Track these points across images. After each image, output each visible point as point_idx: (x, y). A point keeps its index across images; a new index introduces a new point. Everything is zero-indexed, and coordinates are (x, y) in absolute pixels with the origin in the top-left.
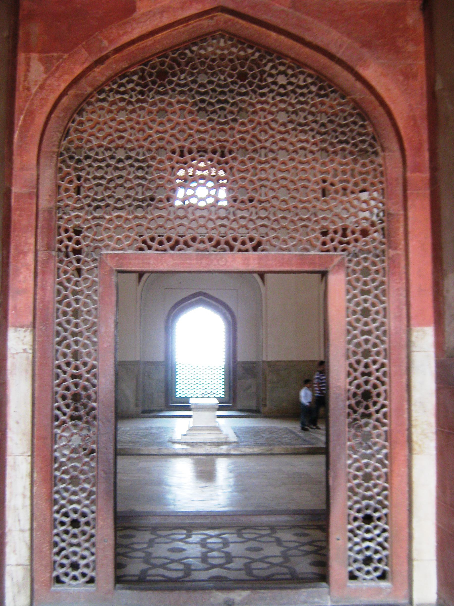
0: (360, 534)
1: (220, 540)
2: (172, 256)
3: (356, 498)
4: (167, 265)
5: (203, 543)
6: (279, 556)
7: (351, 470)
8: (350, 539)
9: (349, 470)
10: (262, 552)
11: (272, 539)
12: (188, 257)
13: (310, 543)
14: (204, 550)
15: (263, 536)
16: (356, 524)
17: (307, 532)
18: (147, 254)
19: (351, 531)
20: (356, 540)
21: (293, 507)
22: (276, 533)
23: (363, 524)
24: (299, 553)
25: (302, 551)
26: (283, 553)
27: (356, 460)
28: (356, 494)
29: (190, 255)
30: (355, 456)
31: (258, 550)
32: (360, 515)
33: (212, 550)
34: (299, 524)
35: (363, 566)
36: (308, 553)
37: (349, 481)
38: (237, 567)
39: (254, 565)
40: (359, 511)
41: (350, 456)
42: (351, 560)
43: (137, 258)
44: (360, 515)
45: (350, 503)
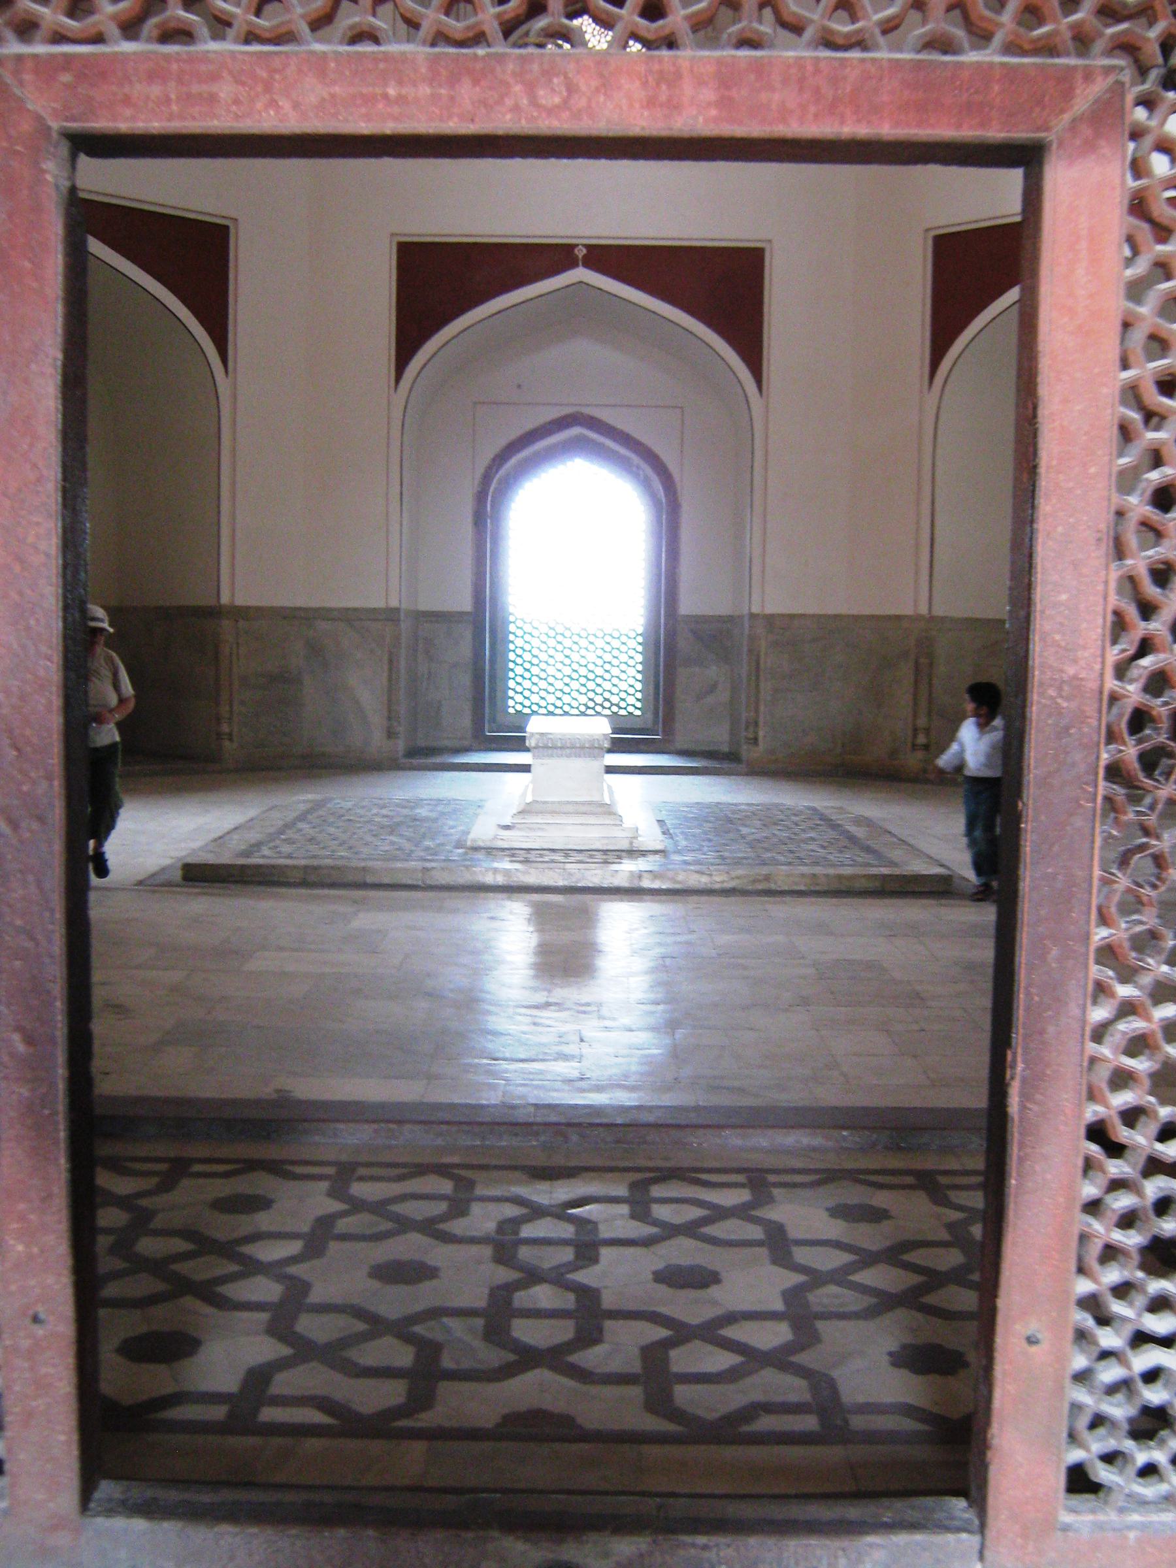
0: (1125, 1319)
1: (567, 1231)
2: (319, 64)
3: (1116, 1168)
4: (296, 106)
5: (503, 1246)
6: (773, 1316)
7: (1105, 1051)
8: (1082, 1336)
9: (1092, 1048)
10: (714, 1291)
11: (755, 1232)
12: (397, 68)
13: (894, 1255)
14: (504, 1275)
15: (720, 1213)
16: (1113, 1275)
17: (881, 1199)
18: (205, 58)
19: (1091, 1303)
20: (1108, 1339)
21: (829, 1096)
22: (771, 1200)
23: (1140, 1274)
24: (854, 1301)
25: (864, 1289)
26: (793, 1296)
27: (1128, 1009)
28: (1115, 1150)
29: (403, 58)
30: (1124, 991)
31: (700, 1279)
32: (1132, 1239)
33: (533, 1277)
34: (850, 1165)
35: (1129, 1445)
36: (886, 1302)
37: (1092, 1095)
38: (616, 1365)
39: (682, 1360)
40: (1128, 1221)
41: (1101, 990)
42: (1083, 1421)
43: (156, 74)
44: (1132, 1239)
45: (1090, 1190)
